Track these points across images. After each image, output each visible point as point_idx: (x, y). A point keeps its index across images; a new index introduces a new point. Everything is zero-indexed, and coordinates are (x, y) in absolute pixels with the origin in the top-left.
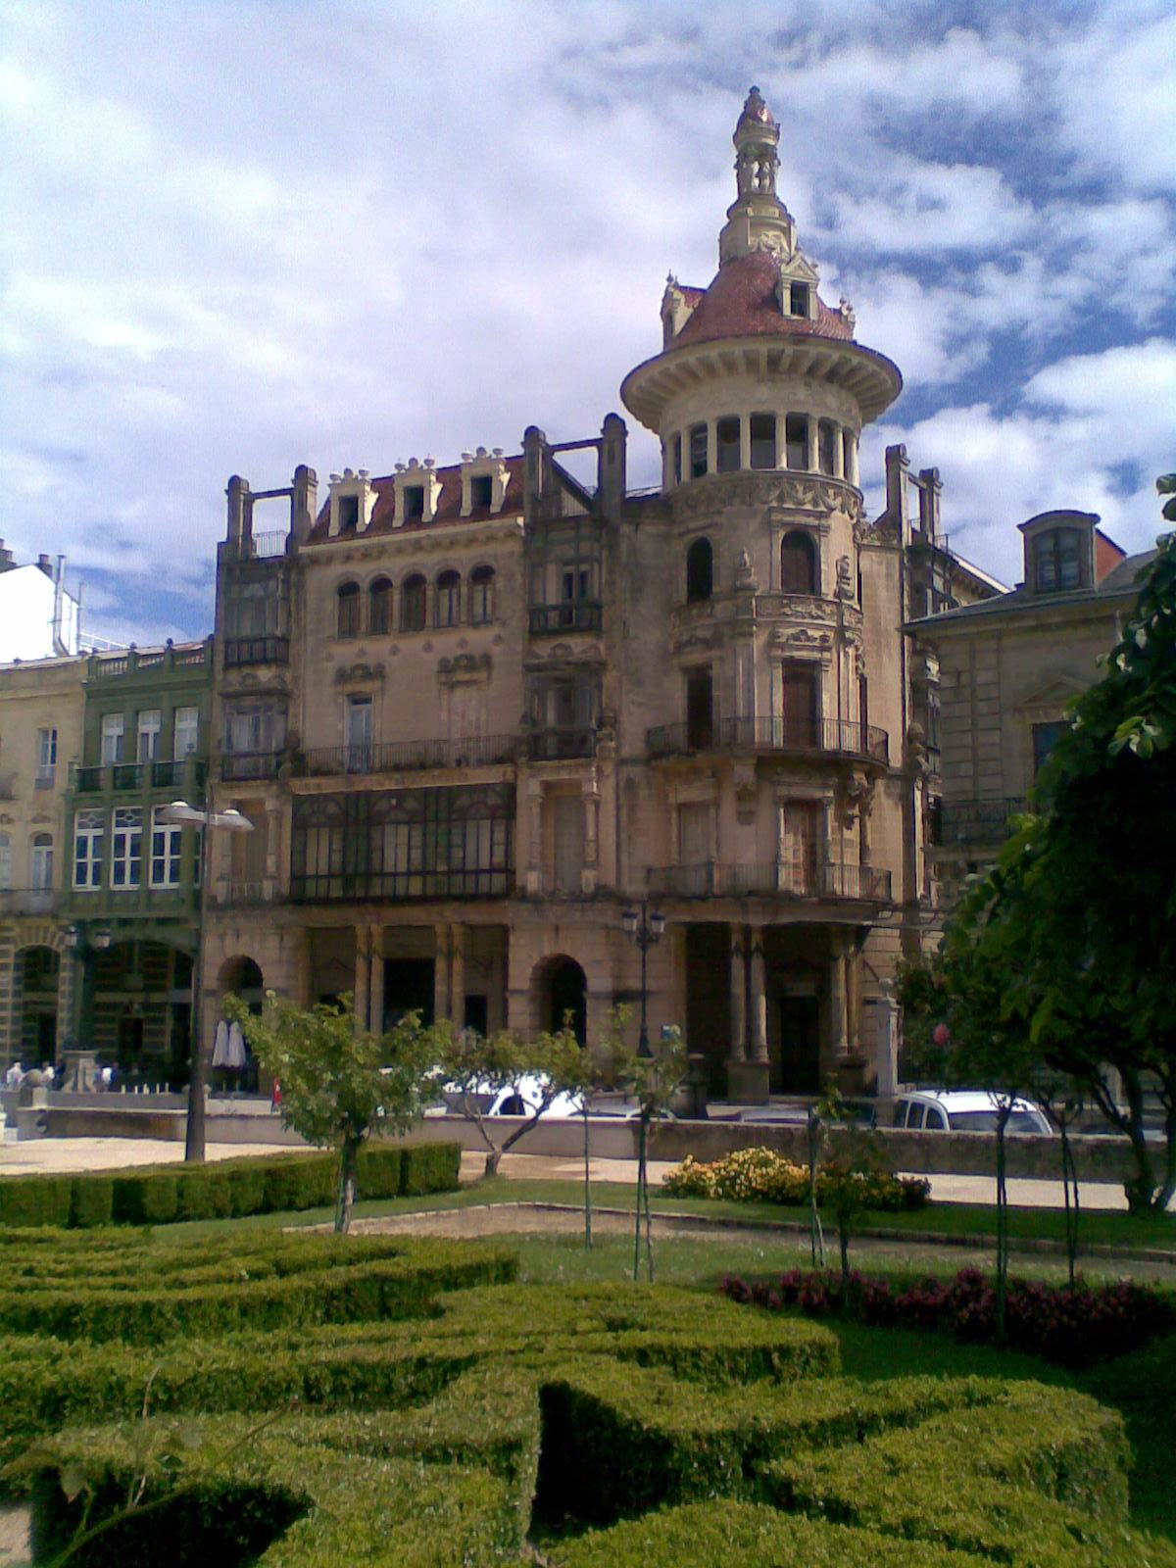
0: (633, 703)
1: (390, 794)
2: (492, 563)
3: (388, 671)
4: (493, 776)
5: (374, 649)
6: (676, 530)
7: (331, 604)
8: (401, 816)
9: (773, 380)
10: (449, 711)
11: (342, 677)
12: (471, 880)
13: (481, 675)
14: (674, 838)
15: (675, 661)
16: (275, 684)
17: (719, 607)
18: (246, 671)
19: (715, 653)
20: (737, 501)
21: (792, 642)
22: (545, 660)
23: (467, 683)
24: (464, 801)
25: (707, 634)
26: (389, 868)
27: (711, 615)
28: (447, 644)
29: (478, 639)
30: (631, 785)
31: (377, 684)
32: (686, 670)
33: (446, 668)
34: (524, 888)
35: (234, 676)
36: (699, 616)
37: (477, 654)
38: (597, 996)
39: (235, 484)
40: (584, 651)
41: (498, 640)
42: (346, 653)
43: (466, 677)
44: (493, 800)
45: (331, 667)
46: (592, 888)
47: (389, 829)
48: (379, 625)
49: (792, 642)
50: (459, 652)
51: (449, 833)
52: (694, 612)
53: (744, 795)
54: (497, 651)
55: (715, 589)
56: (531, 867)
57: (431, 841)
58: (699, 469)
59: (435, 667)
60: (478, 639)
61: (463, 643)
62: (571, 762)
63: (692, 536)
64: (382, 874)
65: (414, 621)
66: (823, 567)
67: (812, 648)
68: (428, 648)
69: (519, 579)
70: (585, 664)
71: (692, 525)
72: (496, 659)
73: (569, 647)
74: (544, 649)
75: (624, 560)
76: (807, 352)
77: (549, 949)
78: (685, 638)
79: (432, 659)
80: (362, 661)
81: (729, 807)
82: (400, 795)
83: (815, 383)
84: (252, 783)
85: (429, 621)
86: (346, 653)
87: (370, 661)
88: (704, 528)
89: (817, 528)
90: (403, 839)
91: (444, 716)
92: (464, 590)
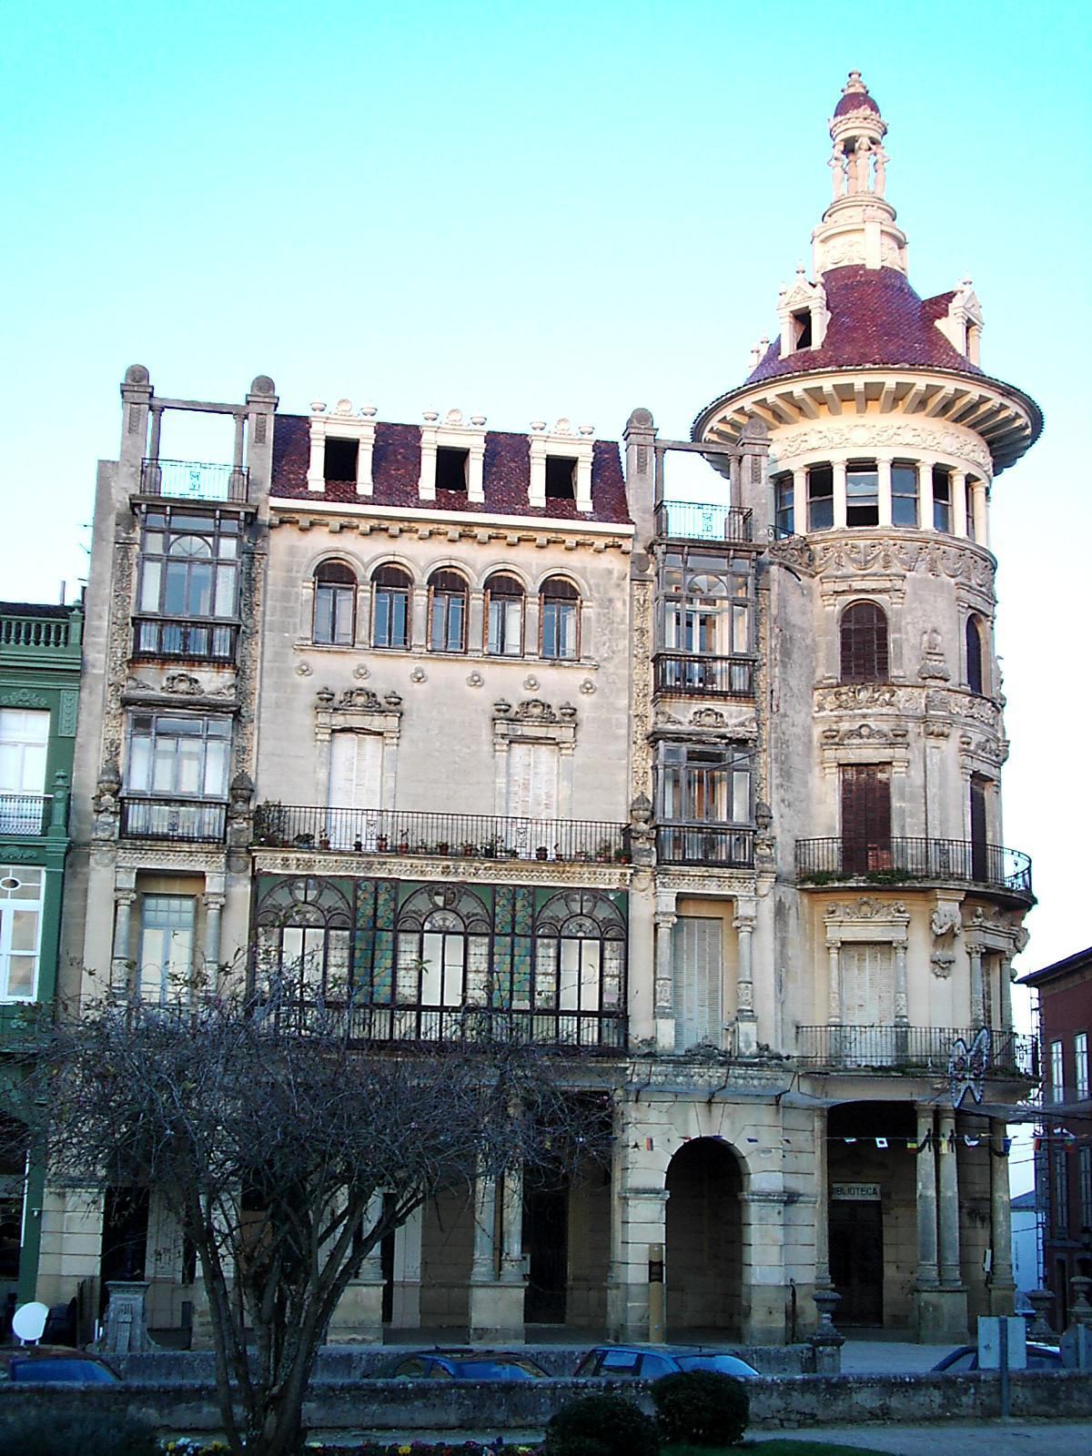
0: (783, 801)
1: (432, 888)
2: (581, 584)
3: (405, 705)
4: (609, 878)
5: (388, 672)
6: (829, 587)
7: (306, 591)
8: (451, 921)
10: (508, 774)
11: (326, 701)
12: (406, 1022)
13: (564, 733)
14: (834, 984)
15: (830, 754)
16: (230, 696)
17: (901, 694)
18: (175, 670)
19: (899, 753)
21: (979, 751)
22: (686, 728)
23: (537, 740)
24: (558, 909)
25: (885, 727)
26: (430, 999)
27: (889, 704)
28: (509, 682)
29: (557, 684)
30: (780, 910)
31: (392, 722)
32: (843, 766)
33: (503, 712)
34: (651, 1042)
35: (154, 681)
37: (555, 703)
38: (766, 1197)
39: (137, 385)
40: (742, 724)
41: (588, 688)
42: (337, 670)
43: (541, 732)
44: (603, 912)
45: (307, 690)
46: (754, 1048)
47: (432, 941)
48: (395, 635)
50: (529, 695)
51: (533, 956)
52: (863, 695)
53: (945, 938)
54: (584, 703)
56: (658, 1014)
57: (502, 962)
58: (863, 516)
59: (492, 711)
60: (557, 684)
61: (532, 684)
62: (727, 872)
63: (855, 597)
64: (419, 1008)
65: (454, 642)
68: (476, 681)
69: (621, 609)
70: (741, 743)
71: (857, 585)
72: (580, 715)
73: (721, 716)
74: (684, 714)
75: (774, 611)
77: (697, 1128)
78: (845, 726)
79: (484, 699)
80: (361, 683)
81: (920, 951)
82: (454, 893)
84: (186, 847)
85: (474, 643)
86: (337, 670)
87: (380, 688)
88: (874, 591)
90: (454, 955)
91: (501, 782)
92: (533, 608)
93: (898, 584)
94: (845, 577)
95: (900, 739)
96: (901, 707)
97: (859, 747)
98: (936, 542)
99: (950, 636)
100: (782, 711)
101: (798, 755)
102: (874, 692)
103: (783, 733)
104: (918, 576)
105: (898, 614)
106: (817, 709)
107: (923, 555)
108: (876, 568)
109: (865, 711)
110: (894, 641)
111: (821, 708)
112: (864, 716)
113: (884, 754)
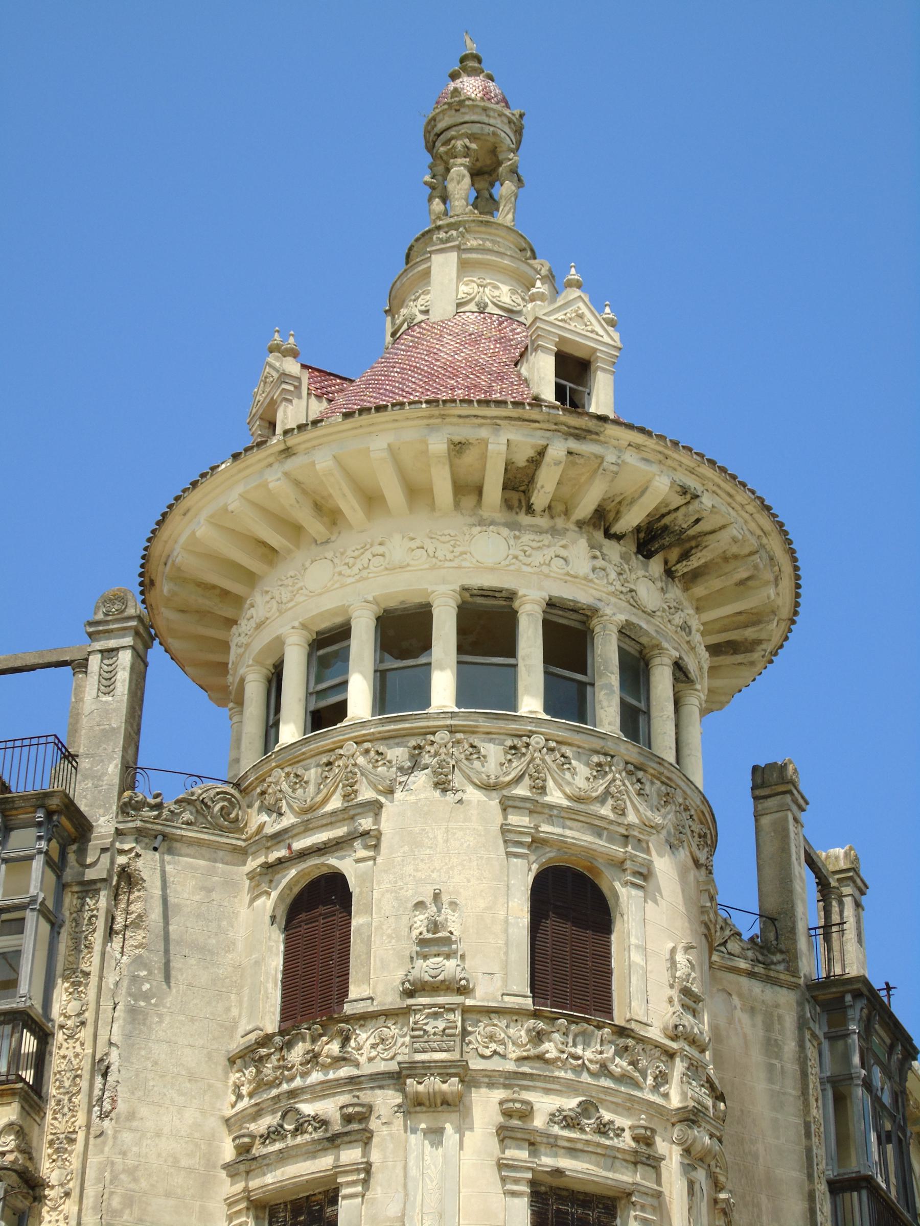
9: (513, 526)
17: (364, 1037)
19: (351, 1155)
20: (421, 779)
21: (556, 1130)
36: (313, 1059)
49: (556, 1130)
55: (354, 992)
66: (636, 957)
67: (610, 1157)
76: (601, 458)
83: (613, 550)
89: (619, 865)
93: (366, 823)
94: (278, 838)
95: (355, 1126)
96: (362, 1060)
97: (283, 1157)
98: (452, 730)
99: (482, 904)
100: (121, 1106)
101: (168, 1195)
102: (314, 1040)
103: (124, 1154)
104: (412, 798)
105: (367, 879)
106: (233, 1098)
107: (426, 759)
108: (335, 803)
109: (298, 1082)
110: (358, 929)
111: (240, 1097)
112: (293, 1094)
113: (324, 1163)
